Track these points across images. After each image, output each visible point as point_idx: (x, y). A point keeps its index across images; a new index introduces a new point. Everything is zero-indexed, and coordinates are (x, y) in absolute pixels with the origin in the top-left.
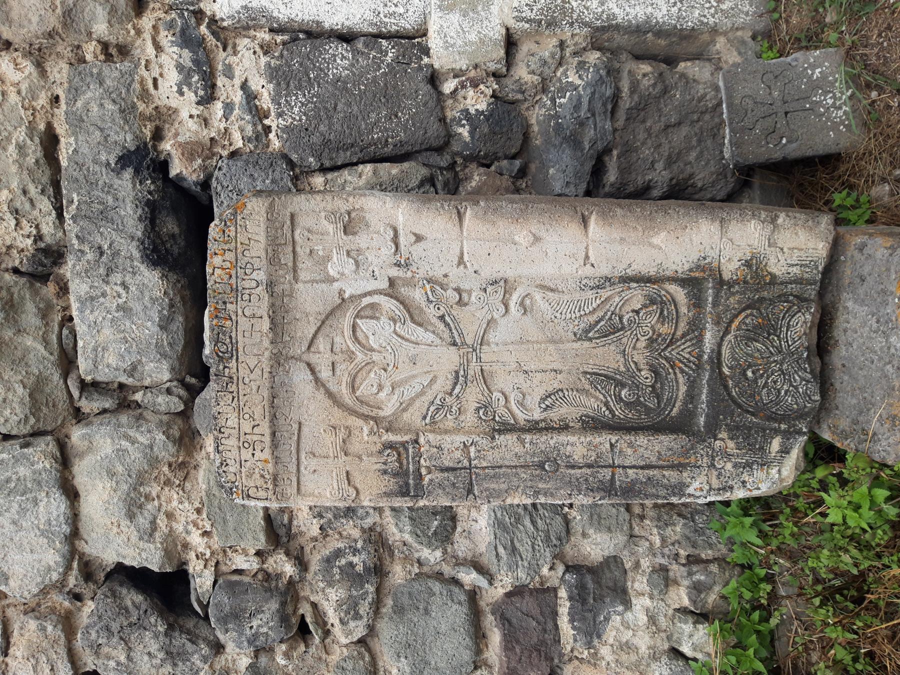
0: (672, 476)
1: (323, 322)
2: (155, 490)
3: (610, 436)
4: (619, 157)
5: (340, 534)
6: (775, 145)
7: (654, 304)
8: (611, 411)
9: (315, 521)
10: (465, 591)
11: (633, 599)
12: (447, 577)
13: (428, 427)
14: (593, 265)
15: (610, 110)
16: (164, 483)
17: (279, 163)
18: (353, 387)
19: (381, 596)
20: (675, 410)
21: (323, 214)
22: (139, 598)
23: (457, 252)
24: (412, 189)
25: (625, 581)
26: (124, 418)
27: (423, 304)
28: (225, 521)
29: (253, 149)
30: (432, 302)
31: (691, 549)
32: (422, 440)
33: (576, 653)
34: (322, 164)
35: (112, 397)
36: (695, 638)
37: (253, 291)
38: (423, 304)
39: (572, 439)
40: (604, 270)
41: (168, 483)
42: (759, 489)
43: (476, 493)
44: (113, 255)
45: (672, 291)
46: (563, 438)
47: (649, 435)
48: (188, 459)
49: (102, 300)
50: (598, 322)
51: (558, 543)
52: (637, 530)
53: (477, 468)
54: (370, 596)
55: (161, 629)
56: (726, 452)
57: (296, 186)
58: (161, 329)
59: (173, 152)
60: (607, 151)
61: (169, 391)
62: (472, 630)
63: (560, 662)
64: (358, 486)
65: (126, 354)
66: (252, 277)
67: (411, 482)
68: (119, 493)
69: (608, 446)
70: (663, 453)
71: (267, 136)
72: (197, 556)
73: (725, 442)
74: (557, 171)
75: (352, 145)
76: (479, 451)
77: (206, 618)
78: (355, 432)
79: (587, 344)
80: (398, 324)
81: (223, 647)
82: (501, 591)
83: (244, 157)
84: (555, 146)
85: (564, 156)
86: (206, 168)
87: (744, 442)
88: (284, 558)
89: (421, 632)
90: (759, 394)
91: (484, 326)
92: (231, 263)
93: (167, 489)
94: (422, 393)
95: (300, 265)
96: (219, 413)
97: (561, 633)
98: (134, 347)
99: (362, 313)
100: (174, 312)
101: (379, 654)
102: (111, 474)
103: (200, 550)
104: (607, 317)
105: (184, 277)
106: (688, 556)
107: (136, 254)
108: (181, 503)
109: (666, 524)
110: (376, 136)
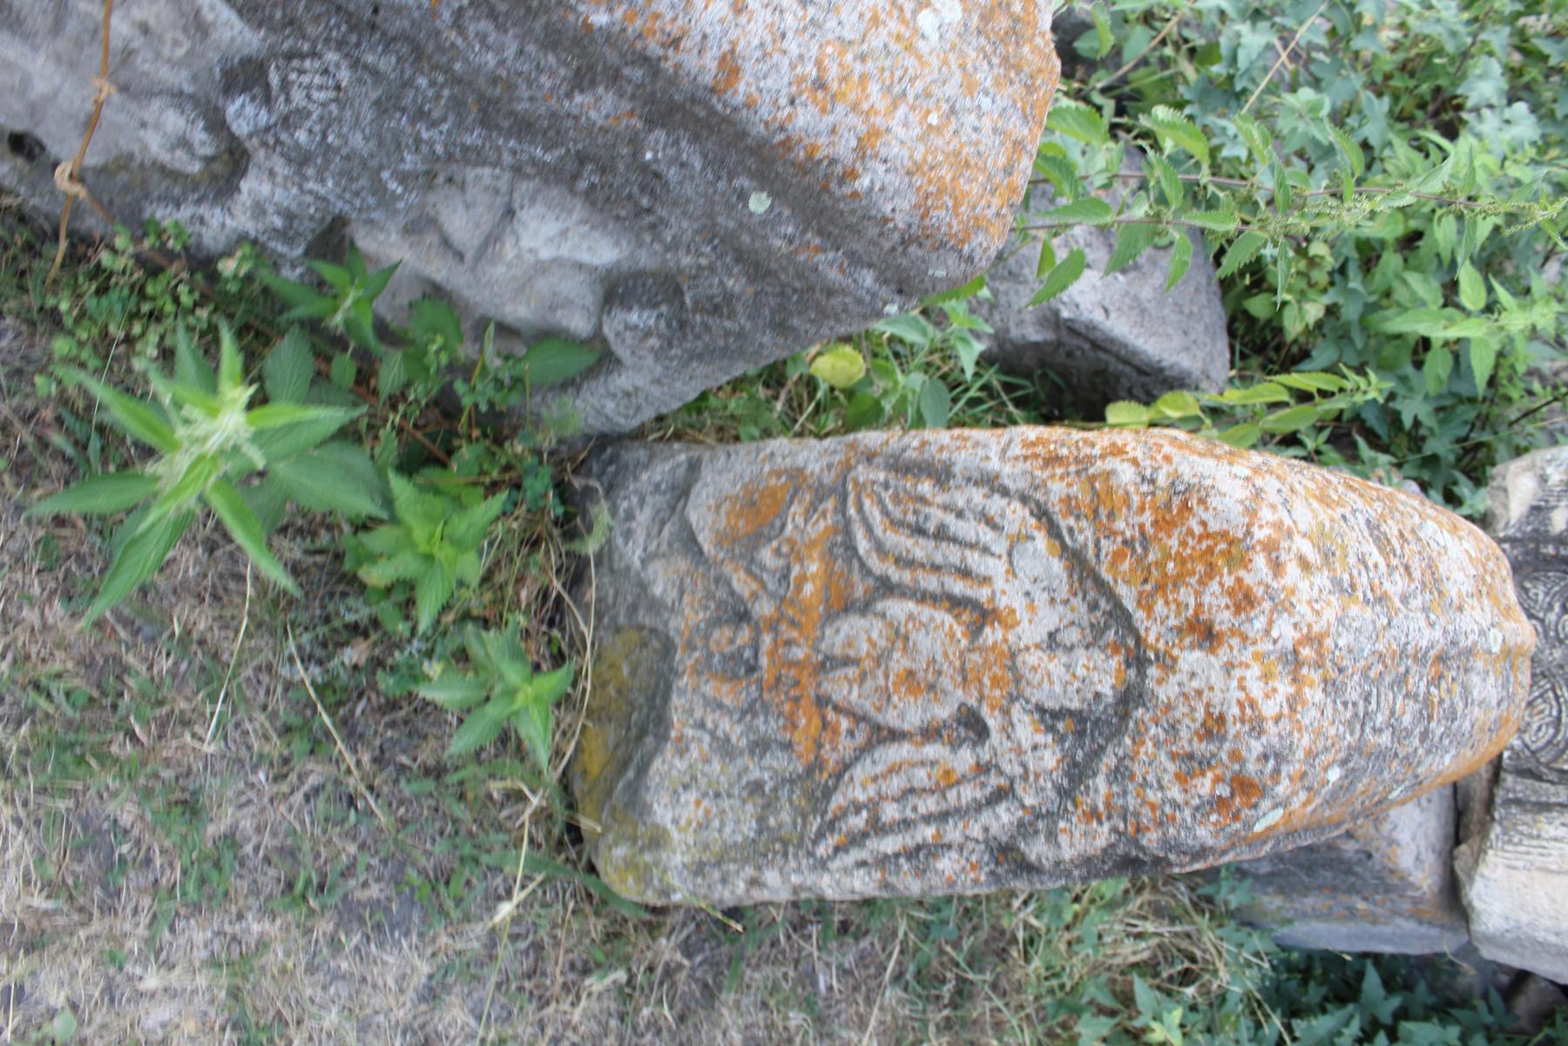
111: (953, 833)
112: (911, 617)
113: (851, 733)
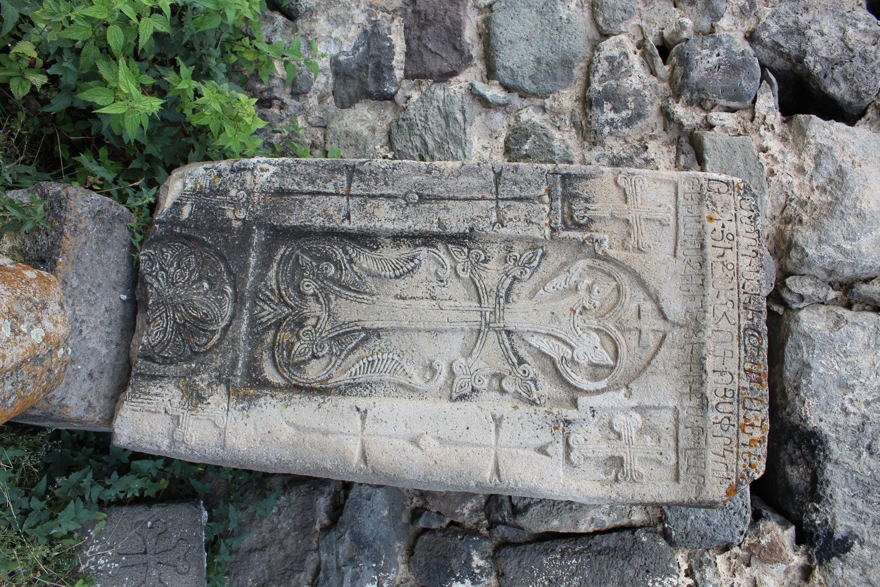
0: (289, 184)
1: (649, 363)
2: (816, 197)
3: (349, 227)
4: (314, 522)
5: (626, 142)
6: (159, 520)
7: (296, 364)
8: (346, 253)
9: (653, 156)
10: (498, 79)
11: (329, 67)
12: (516, 95)
13: (540, 244)
14: (358, 410)
15: (321, 573)
16: (806, 203)
17: (679, 537)
18: (619, 291)
19: (584, 78)
20: (282, 252)
21: (645, 481)
22: (832, 90)
23: (502, 432)
24: (537, 503)
25: (334, 84)
26: (848, 272)
27: (540, 377)
28: (745, 161)
29: (706, 553)
30: (531, 380)
31: (267, 113)
32: (547, 231)
33: (389, 17)
34: (633, 534)
35: (860, 295)
36: (270, 29)
37: (722, 400)
38: (540, 377)
39: (389, 226)
40: (346, 403)
41: (803, 204)
42: (206, 169)
43: (492, 173)
44: (857, 445)
45: (278, 376)
46: (398, 226)
48: (782, 227)
49: (870, 398)
50: (355, 348)
51: (401, 122)
52: (319, 134)
53: (490, 199)
54: (596, 79)
55: (809, 59)
56: (234, 206)
57: (662, 511)
58: (809, 364)
59: (791, 553)
60: (326, 529)
61: (801, 298)
62: (493, 41)
63: (405, 10)
64: (615, 188)
65: (845, 340)
66: (723, 415)
67: (560, 189)
68: (853, 196)
69: (352, 217)
71: (690, 566)
72: (773, 128)
73: (236, 217)
74: (379, 513)
75: (599, 553)
76: (487, 217)
77: (763, 67)
78: (618, 244)
79: (368, 325)
80: (569, 357)
81: (746, 37)
82: (461, 77)
83: (715, 545)
84: (381, 539)
85: (371, 528)
86: (756, 534)
88: (684, 121)
89: (546, 42)
90: (198, 263)
91: (475, 351)
92: (743, 431)
93: (804, 198)
94: (544, 282)
95: (671, 426)
96: (758, 272)
97: (403, 36)
98: (837, 347)
99: (607, 371)
100: (795, 381)
101: (588, 23)
102: (861, 215)
103: (769, 134)
104: (345, 352)
105: (782, 419)
106: (270, 107)
107: (833, 445)
108: (790, 183)
109: (290, 138)
110: (574, 561)
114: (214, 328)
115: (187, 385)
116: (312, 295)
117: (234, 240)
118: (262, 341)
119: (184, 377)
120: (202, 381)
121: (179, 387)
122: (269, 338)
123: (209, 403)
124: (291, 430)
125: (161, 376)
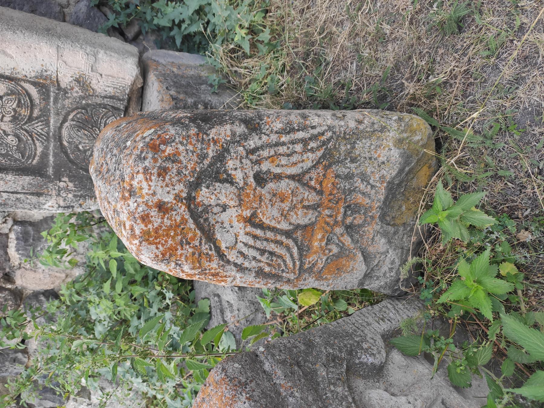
0: (34, 199)
7: (14, 94)
42: (90, 208)
47: (16, 175)
70: (25, 186)
73: (65, 182)
87: (79, 184)
97: (10, 256)
111: (274, 138)
112: (279, 222)
113: (311, 179)
114: (72, 123)
115: (87, 90)
116: (9, 135)
117: (65, 171)
118: (41, 110)
119: (90, 95)
120: (77, 92)
121: (93, 90)
122: (36, 113)
123: (72, 77)
124: (8, 51)
125: (106, 98)
